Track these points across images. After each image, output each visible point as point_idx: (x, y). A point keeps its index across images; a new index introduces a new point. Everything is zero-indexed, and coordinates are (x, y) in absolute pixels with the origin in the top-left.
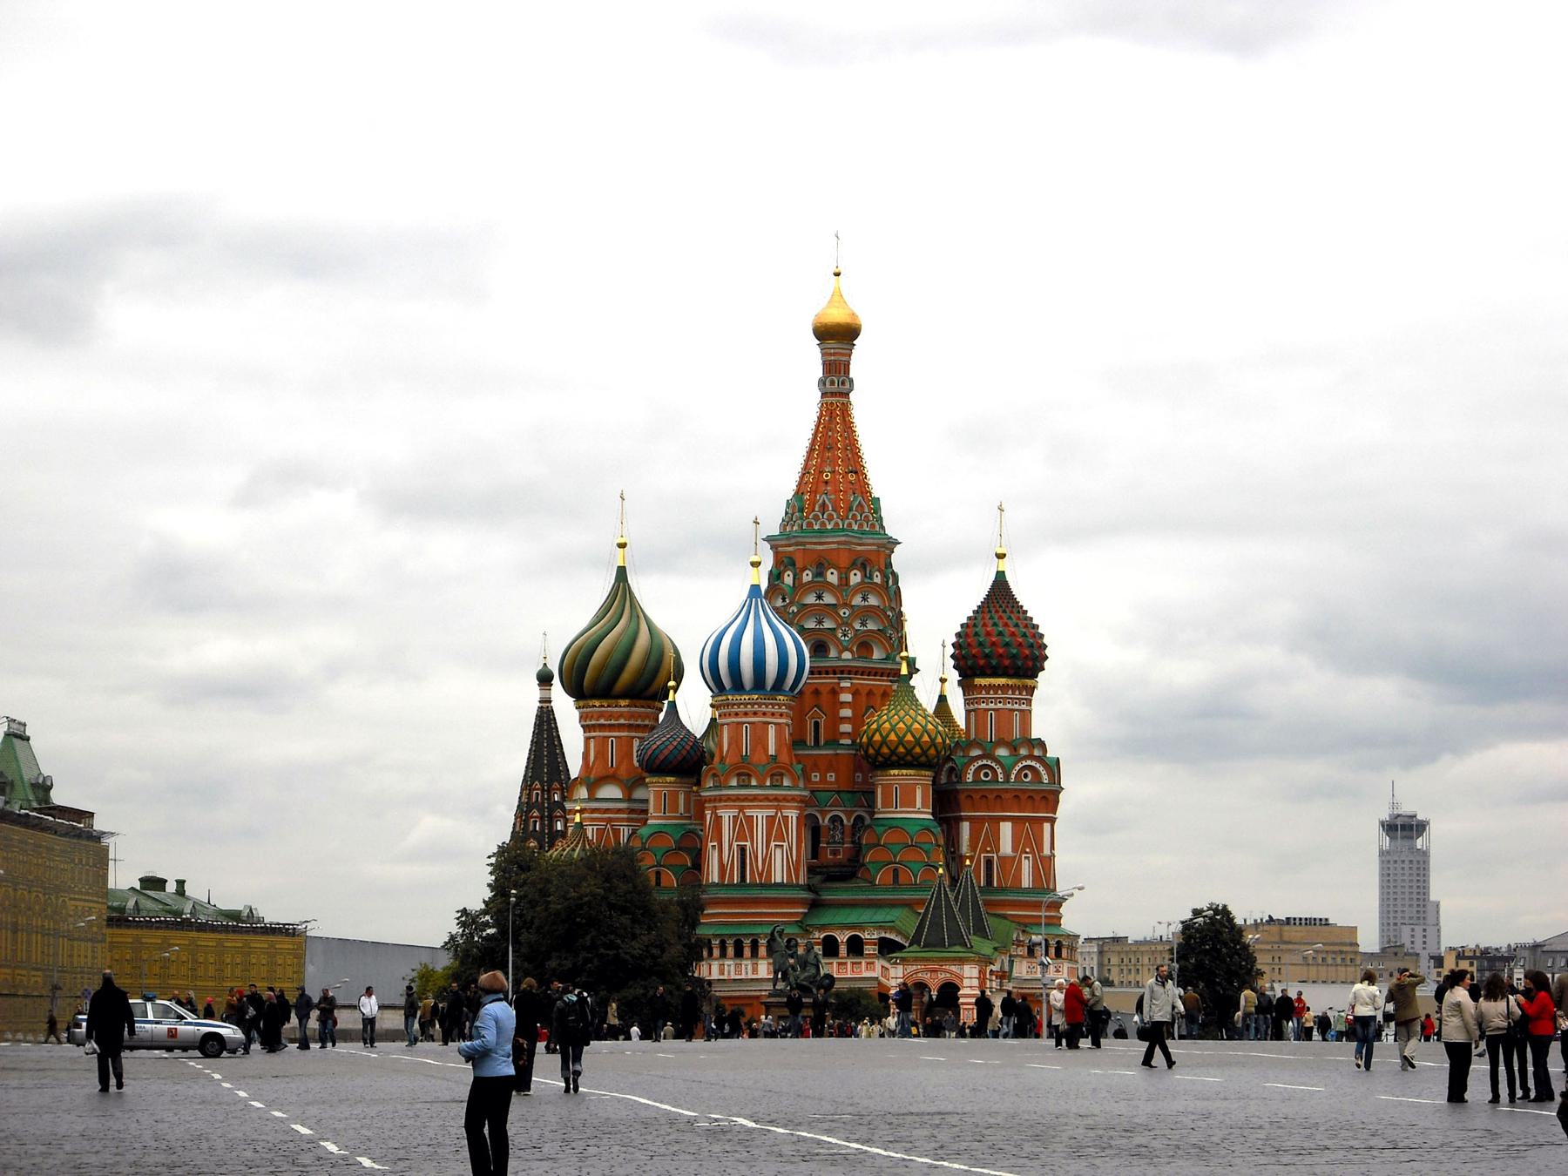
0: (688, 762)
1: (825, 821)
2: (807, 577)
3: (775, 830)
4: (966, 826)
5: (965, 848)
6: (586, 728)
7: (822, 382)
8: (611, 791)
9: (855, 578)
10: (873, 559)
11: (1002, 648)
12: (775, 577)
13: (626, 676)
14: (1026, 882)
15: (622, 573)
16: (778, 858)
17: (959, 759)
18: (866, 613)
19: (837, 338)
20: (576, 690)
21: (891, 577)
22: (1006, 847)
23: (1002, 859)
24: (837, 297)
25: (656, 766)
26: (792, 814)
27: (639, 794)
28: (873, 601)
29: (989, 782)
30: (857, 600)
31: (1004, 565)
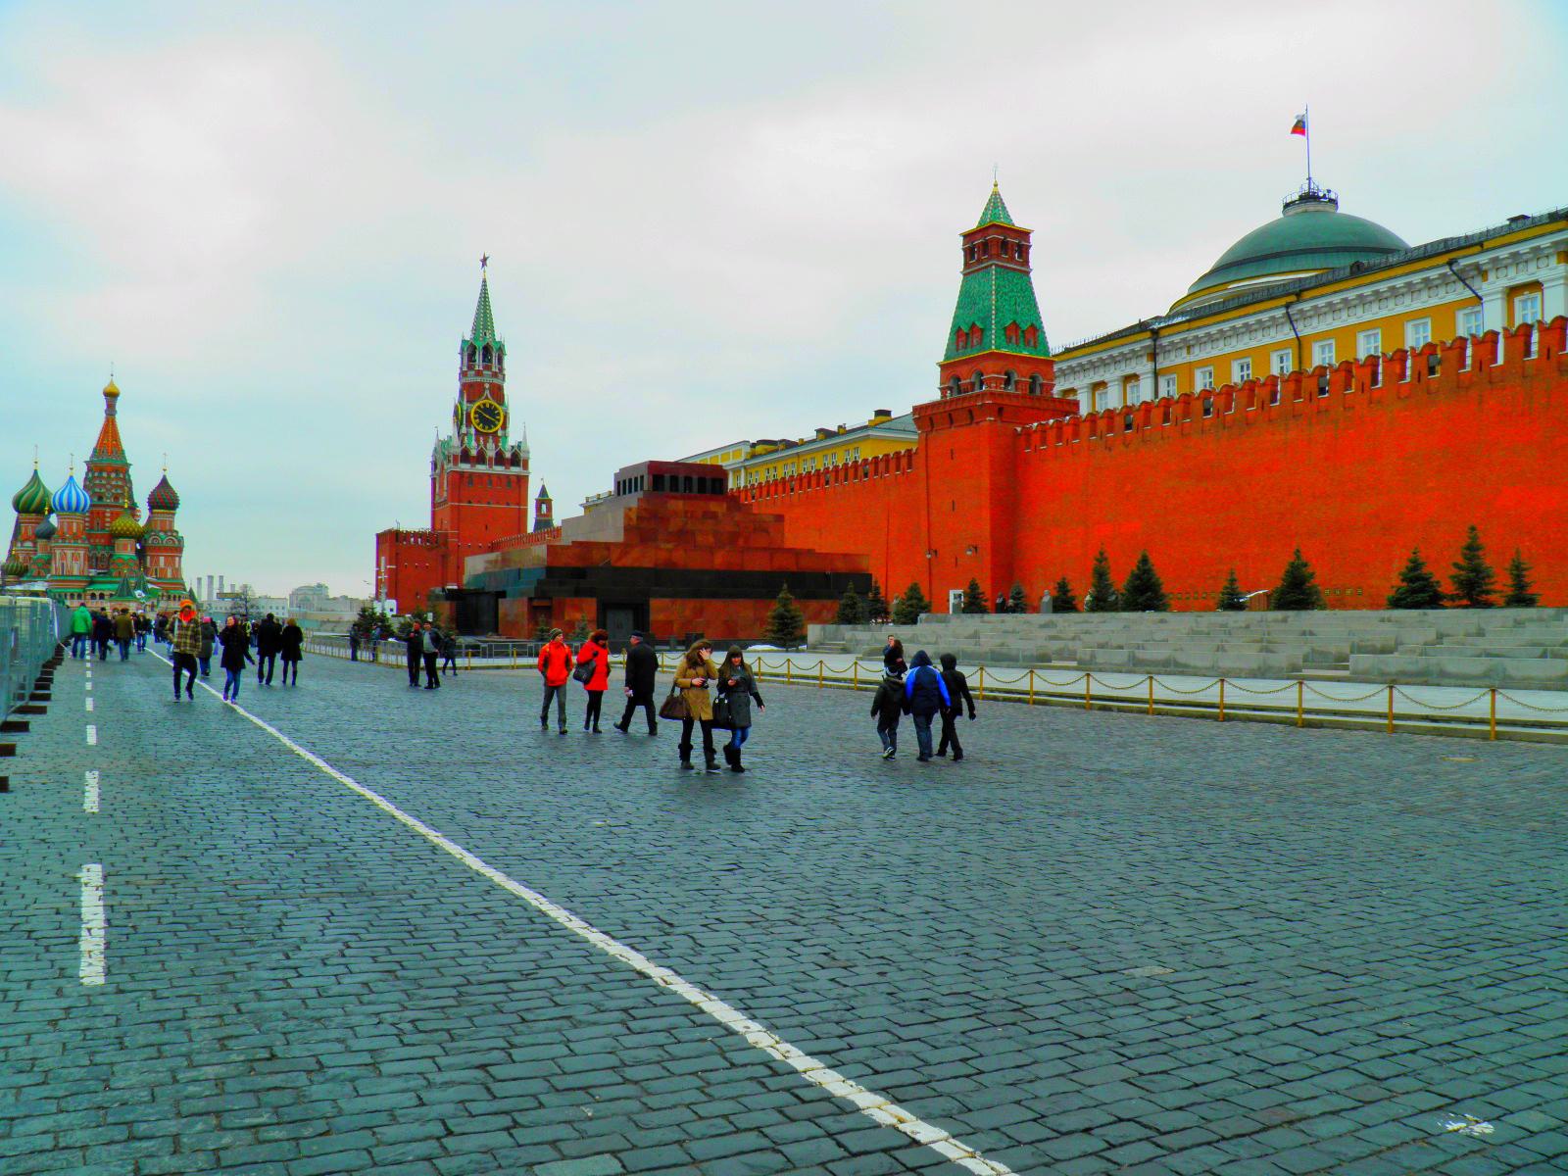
0: (48, 534)
2: (96, 474)
3: (75, 558)
5: (148, 565)
8: (28, 544)
10: (122, 470)
11: (164, 500)
12: (87, 474)
14: (169, 575)
15: (36, 472)
17: (146, 536)
23: (161, 569)
24: (112, 384)
25: (41, 536)
26: (82, 553)
28: (120, 483)
29: (156, 546)
30: (114, 483)
31: (167, 473)
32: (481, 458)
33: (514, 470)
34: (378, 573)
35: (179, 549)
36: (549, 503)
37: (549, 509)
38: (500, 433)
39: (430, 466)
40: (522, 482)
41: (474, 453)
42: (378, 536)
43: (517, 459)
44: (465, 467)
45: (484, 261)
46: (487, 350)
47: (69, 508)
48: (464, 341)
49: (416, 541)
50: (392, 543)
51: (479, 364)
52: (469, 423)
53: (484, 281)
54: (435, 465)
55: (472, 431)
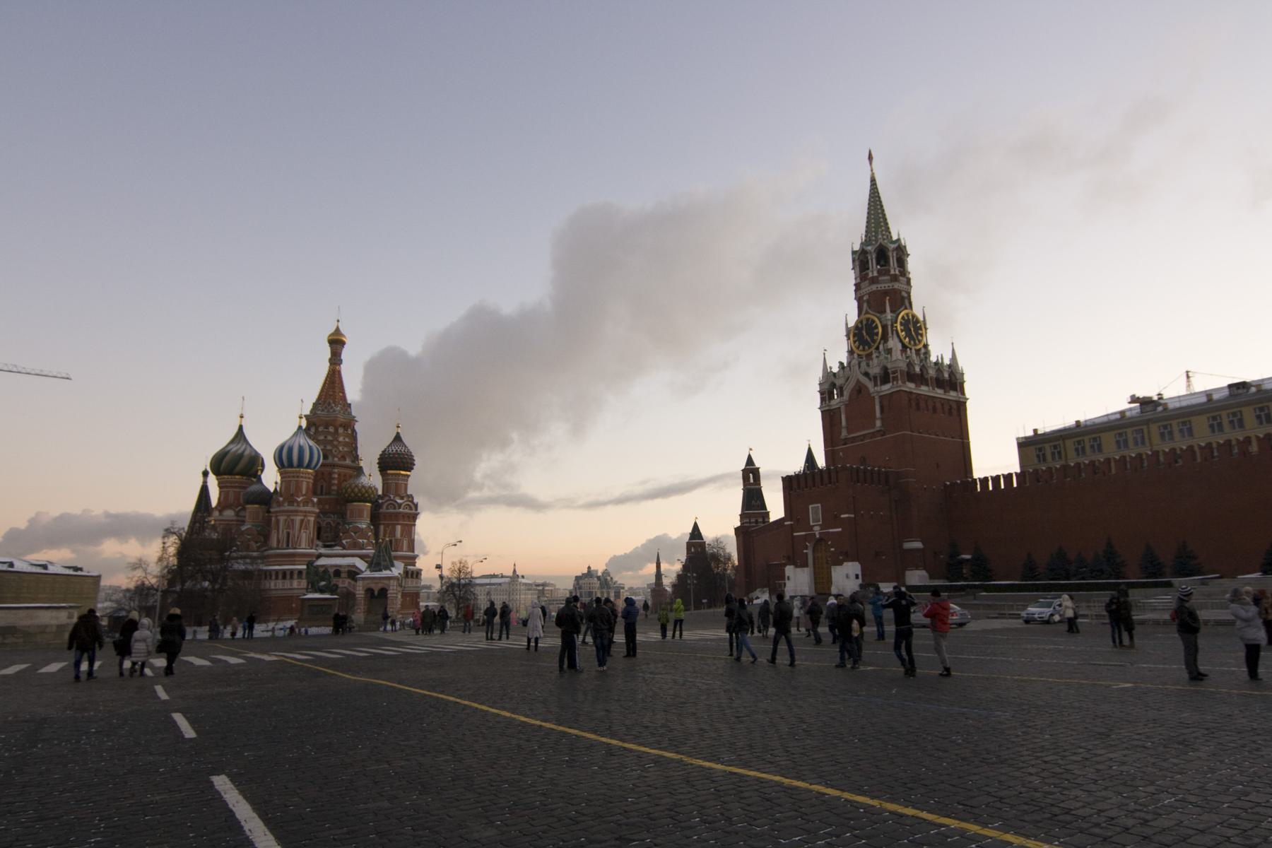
0: (265, 498)
1: (324, 525)
2: (321, 429)
4: (382, 527)
6: (220, 487)
7: (330, 360)
9: (341, 430)
13: (238, 468)
15: (241, 428)
16: (304, 535)
18: (346, 444)
19: (336, 343)
20: (217, 472)
21: (354, 431)
22: (398, 534)
26: (312, 519)
27: (242, 513)
30: (341, 439)
32: (920, 379)
33: (953, 395)
39: (818, 396)
40: (958, 411)
41: (917, 369)
43: (951, 379)
44: (911, 386)
45: (870, 158)
47: (300, 465)
51: (894, 270)
53: (873, 181)
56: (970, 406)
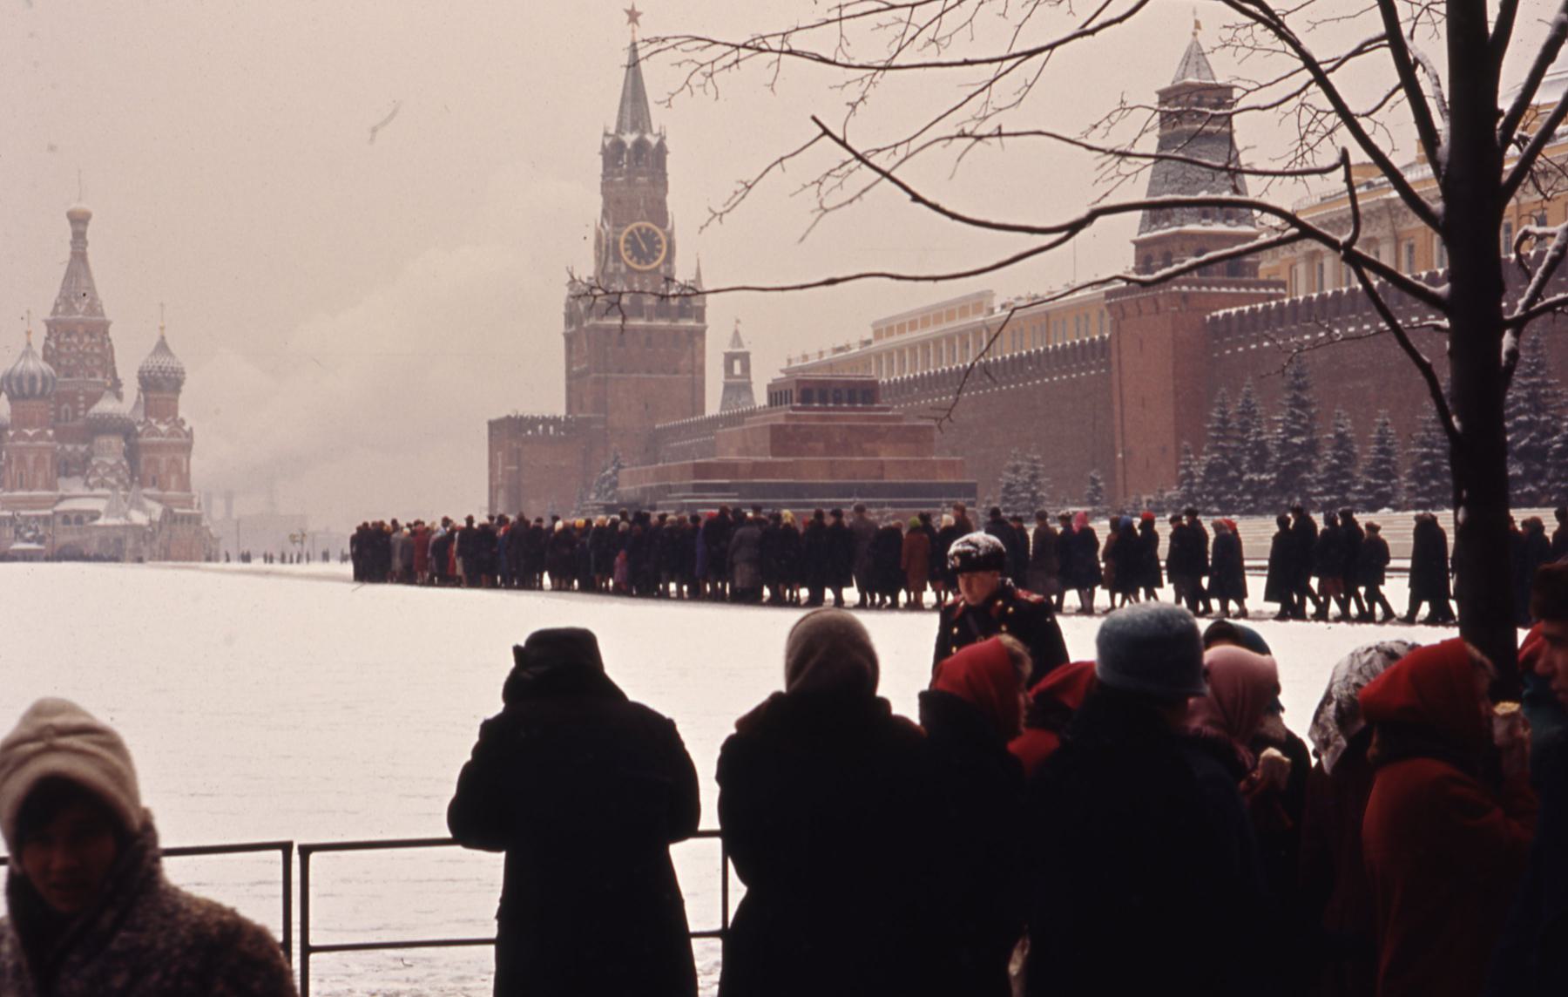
10: (99, 329)
34: (492, 477)
35: (187, 448)
36: (745, 358)
37: (746, 368)
38: (662, 270)
42: (494, 426)
46: (641, 145)
48: (606, 135)
49: (546, 430)
50: (510, 434)
52: (618, 258)
54: (570, 318)
55: (623, 269)
56: (708, 332)
